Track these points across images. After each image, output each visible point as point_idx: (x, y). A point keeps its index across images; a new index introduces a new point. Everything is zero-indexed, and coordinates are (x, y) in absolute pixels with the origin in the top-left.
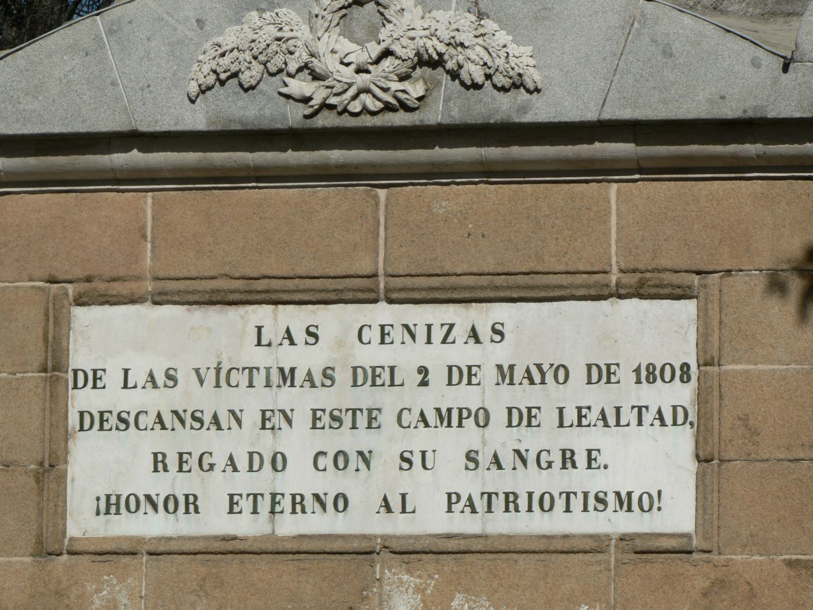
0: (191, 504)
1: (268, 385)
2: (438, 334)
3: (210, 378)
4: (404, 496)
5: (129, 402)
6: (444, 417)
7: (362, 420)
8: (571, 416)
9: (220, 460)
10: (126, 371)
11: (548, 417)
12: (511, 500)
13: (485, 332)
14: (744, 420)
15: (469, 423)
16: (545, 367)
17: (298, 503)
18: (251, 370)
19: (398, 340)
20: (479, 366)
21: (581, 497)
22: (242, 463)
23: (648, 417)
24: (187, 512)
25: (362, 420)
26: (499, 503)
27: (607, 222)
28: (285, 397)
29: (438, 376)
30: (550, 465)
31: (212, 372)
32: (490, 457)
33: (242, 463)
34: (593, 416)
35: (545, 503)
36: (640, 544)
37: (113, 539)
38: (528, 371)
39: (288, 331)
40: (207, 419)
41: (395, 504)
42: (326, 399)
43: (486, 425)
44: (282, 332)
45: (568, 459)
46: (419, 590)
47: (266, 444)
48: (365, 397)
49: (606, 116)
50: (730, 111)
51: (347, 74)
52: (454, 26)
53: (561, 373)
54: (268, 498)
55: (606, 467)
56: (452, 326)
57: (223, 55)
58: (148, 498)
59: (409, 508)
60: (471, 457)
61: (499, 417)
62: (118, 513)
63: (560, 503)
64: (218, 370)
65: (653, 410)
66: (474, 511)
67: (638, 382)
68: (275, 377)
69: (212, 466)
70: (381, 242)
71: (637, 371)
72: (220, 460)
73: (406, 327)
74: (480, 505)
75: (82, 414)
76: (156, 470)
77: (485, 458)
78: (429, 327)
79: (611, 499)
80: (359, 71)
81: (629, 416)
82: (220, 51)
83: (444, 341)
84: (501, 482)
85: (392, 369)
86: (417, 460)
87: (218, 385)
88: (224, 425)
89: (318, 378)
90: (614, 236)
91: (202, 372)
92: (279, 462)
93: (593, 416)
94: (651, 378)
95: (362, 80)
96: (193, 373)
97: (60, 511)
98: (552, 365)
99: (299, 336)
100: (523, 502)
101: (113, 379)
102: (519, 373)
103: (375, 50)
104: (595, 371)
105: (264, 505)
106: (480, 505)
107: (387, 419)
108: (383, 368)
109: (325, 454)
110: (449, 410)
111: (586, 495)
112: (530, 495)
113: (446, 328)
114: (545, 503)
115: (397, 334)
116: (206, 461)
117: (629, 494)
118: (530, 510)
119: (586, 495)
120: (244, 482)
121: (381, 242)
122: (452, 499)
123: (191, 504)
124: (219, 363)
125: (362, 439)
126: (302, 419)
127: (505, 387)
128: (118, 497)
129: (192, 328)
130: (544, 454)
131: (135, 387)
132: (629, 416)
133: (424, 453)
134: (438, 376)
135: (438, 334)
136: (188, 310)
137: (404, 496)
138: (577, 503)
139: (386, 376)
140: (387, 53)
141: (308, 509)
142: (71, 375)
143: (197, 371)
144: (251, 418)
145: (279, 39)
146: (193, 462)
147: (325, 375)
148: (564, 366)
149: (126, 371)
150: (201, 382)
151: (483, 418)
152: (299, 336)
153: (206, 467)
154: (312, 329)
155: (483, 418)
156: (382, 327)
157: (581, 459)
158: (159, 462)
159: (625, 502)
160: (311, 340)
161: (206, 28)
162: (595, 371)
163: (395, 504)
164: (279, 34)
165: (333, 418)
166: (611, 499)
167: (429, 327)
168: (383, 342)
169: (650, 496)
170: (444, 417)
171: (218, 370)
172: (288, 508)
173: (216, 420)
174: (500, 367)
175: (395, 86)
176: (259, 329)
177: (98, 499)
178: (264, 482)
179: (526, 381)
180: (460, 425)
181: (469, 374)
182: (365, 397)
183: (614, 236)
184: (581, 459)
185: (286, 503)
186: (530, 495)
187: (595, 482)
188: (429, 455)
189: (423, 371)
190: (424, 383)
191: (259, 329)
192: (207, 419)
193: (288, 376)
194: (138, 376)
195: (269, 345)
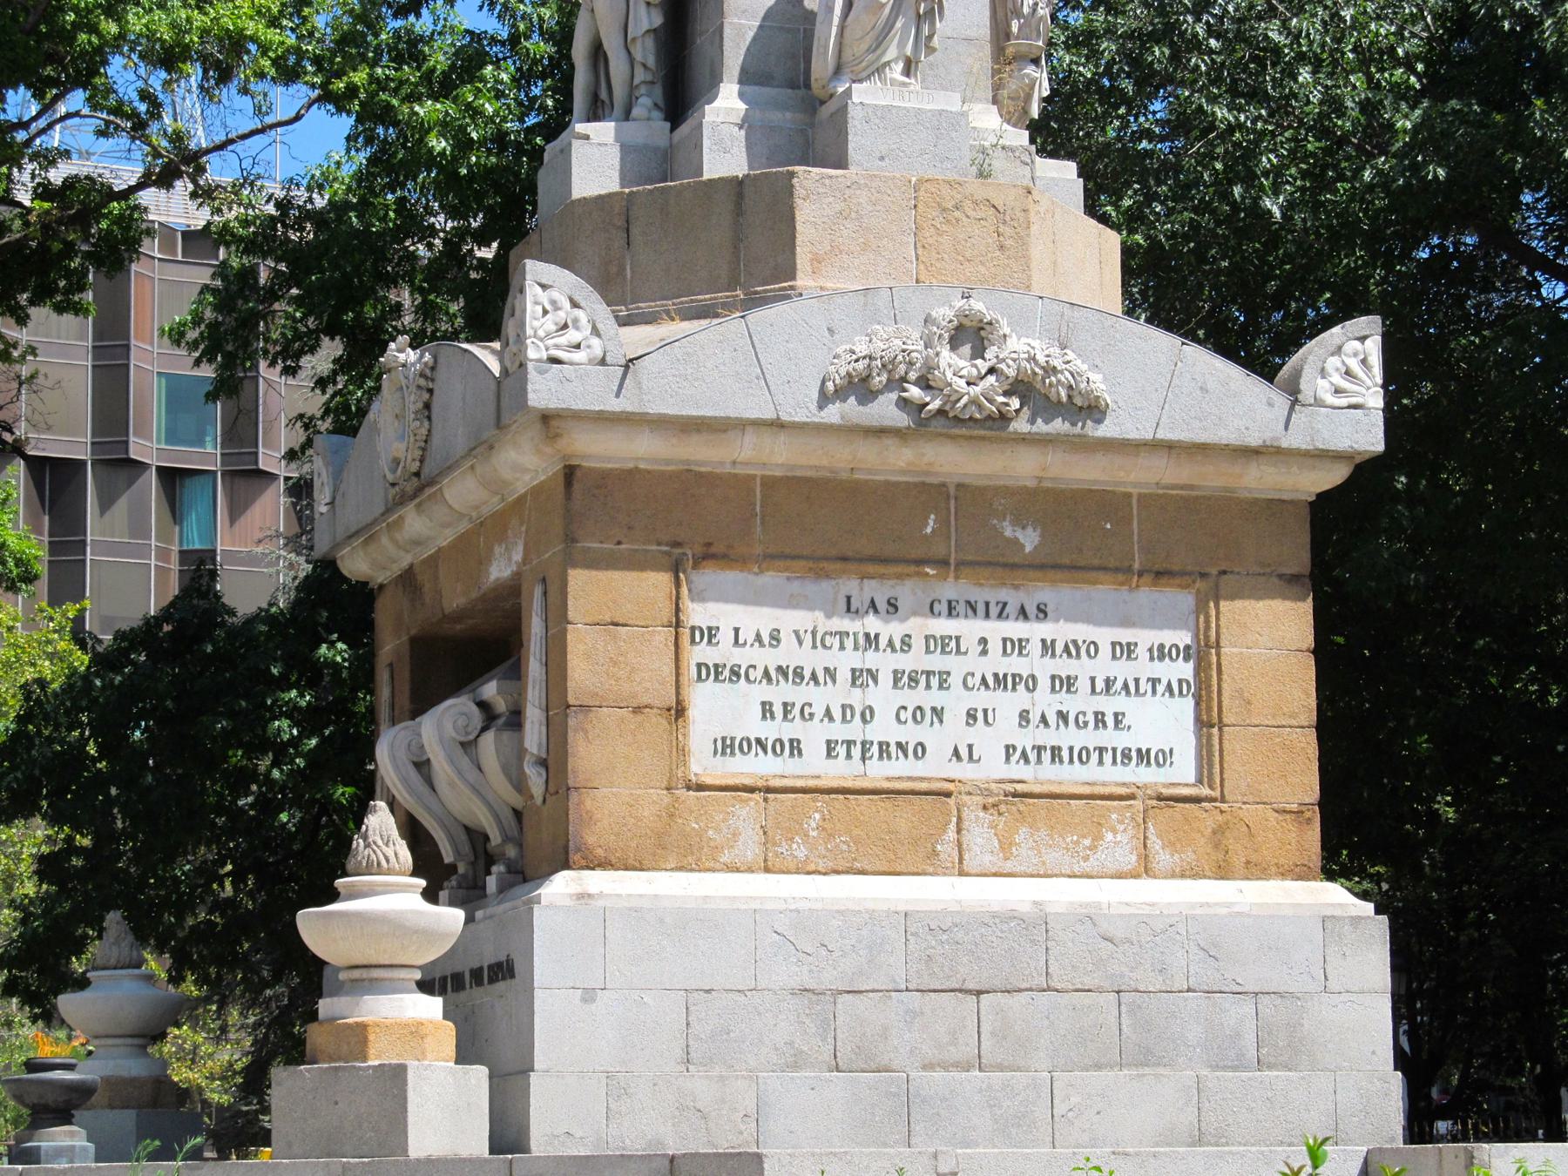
0: (795, 747)
1: (856, 648)
2: (994, 610)
3: (808, 639)
4: (970, 747)
5: (742, 657)
6: (1000, 681)
7: (935, 682)
8: (1100, 685)
9: (819, 711)
10: (737, 630)
11: (1083, 685)
12: (1056, 752)
13: (1031, 610)
14: (1240, 691)
15: (1021, 687)
16: (1080, 643)
17: (884, 748)
18: (840, 633)
19: (962, 612)
20: (1028, 640)
21: (1110, 752)
22: (837, 714)
23: (1161, 688)
24: (792, 754)
25: (935, 682)
26: (1046, 756)
27: (1130, 523)
28: (871, 659)
29: (995, 646)
30: (1086, 724)
31: (809, 636)
32: (1038, 718)
33: (837, 714)
34: (1119, 685)
35: (1083, 756)
36: (1166, 792)
37: (734, 775)
38: (1066, 646)
39: (872, 601)
40: (807, 674)
41: (964, 752)
42: (906, 662)
43: (1034, 689)
44: (867, 603)
45: (1100, 719)
46: (993, 826)
47: (856, 698)
48: (936, 662)
49: (1161, 435)
50: (1254, 440)
51: (962, 382)
52: (1047, 352)
53: (1092, 648)
54: (859, 746)
55: (1129, 727)
56: (1005, 604)
57: (857, 361)
58: (758, 741)
59: (975, 757)
60: (1024, 716)
61: (1044, 683)
62: (733, 754)
63: (1095, 757)
64: (814, 633)
65: (1164, 682)
66: (1027, 761)
67: (1152, 659)
68: (861, 641)
69: (811, 715)
70: (953, 529)
71: (1150, 650)
72: (819, 711)
73: (968, 602)
74: (1032, 756)
75: (699, 666)
76: (764, 717)
77: (1035, 717)
78: (987, 604)
79: (1134, 754)
80: (969, 384)
81: (1145, 686)
82: (854, 357)
83: (1000, 616)
84: (1049, 737)
85: (958, 639)
86: (980, 715)
87: (814, 647)
88: (821, 680)
89: (898, 645)
90: (1136, 538)
91: (802, 633)
92: (867, 715)
93: (1119, 685)
94: (1161, 658)
95: (976, 390)
96: (793, 636)
97: (682, 752)
98: (1084, 642)
99: (882, 605)
100: (1065, 754)
101: (726, 636)
102: (1059, 648)
103: (983, 366)
104: (1009, 645)
105: (856, 752)
106: (1032, 756)
107: (955, 680)
108: (951, 637)
109: (905, 708)
110: (1005, 676)
111: (1114, 750)
112: (1071, 749)
113: (1000, 606)
114: (1083, 756)
115: (961, 608)
116: (807, 710)
117: (1148, 751)
118: (1071, 761)
119: (1114, 750)
120: (839, 731)
121: (953, 529)
122: (1009, 750)
123: (795, 747)
124: (815, 627)
125: (934, 698)
126: (886, 678)
127: (1047, 658)
128: (733, 739)
129: (792, 595)
130: (1081, 716)
131: (745, 643)
132: (1145, 686)
133: (985, 711)
134: (995, 646)
135: (994, 610)
136: (788, 579)
137: (970, 747)
138: (1108, 757)
139: (953, 644)
140: (991, 371)
141: (894, 755)
142: (687, 631)
143: (796, 633)
144: (844, 676)
145: (904, 351)
146: (796, 711)
147: (903, 642)
148: (1093, 643)
149: (737, 630)
150: (800, 643)
151: (1031, 683)
152: (882, 605)
153: (807, 717)
154: (892, 601)
155: (1031, 683)
156: (950, 602)
157: (1110, 721)
158: (767, 709)
159: (1144, 756)
160: (891, 609)
161: (837, 337)
162: (1009, 645)
163: (964, 752)
164: (905, 347)
165: (911, 679)
166: (1134, 754)
167: (987, 604)
168: (950, 614)
169: (1164, 753)
170: (1000, 681)
171: (814, 633)
172: (876, 755)
173: (814, 677)
174: (1043, 641)
175: (1001, 399)
176: (849, 598)
177: (715, 741)
178: (855, 730)
179: (1065, 655)
180: (1014, 688)
181: (1021, 645)
182: (936, 662)
183: (1136, 538)
184: (1110, 721)
185: (875, 749)
186: (1071, 749)
187: (1121, 740)
188: (990, 713)
189: (983, 641)
190: (984, 652)
191: (849, 598)
192: (807, 674)
193: (871, 641)
194: (747, 635)
195: (857, 612)
